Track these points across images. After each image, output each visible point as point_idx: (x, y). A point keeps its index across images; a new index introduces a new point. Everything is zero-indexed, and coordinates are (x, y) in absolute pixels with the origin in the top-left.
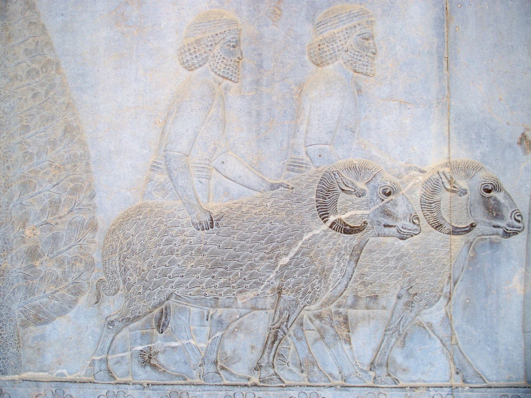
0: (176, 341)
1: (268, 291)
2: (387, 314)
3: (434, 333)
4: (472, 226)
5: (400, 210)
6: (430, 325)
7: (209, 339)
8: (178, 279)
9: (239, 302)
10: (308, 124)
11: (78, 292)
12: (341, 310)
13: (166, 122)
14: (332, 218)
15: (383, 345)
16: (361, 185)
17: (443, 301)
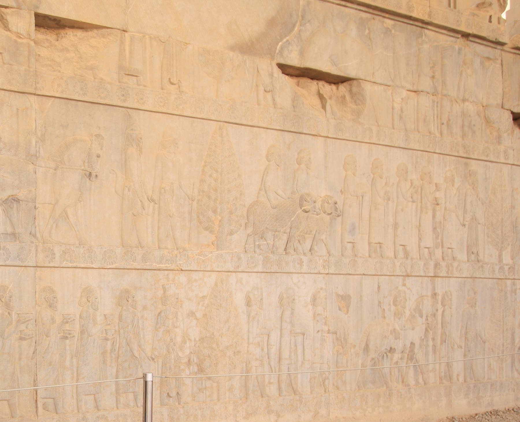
0: (265, 242)
1: (288, 228)
2: (313, 236)
3: (323, 242)
4: (332, 213)
5: (317, 207)
6: (322, 240)
7: (273, 241)
8: (267, 223)
9: (282, 230)
10: (297, 181)
11: (241, 226)
12: (303, 234)
13: (263, 177)
14: (303, 208)
15: (313, 244)
16: (309, 199)
17: (325, 233)
